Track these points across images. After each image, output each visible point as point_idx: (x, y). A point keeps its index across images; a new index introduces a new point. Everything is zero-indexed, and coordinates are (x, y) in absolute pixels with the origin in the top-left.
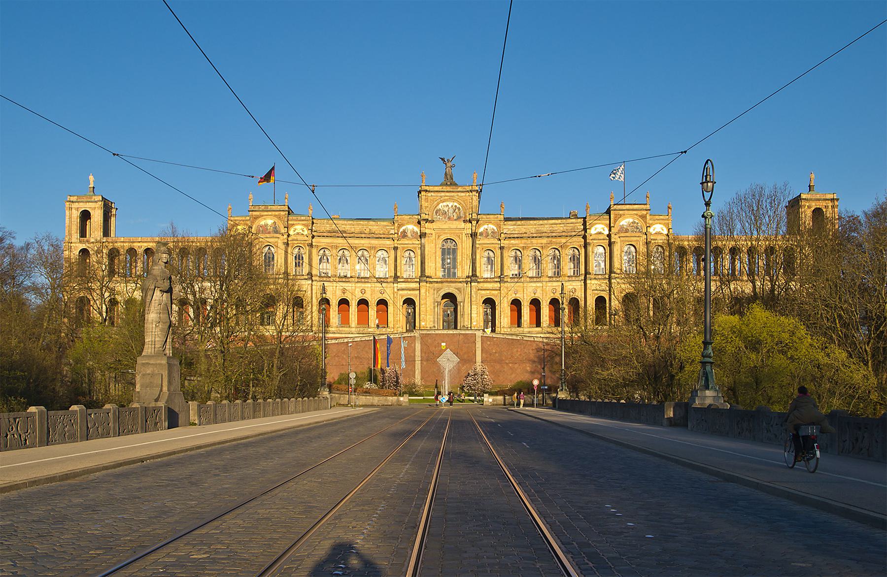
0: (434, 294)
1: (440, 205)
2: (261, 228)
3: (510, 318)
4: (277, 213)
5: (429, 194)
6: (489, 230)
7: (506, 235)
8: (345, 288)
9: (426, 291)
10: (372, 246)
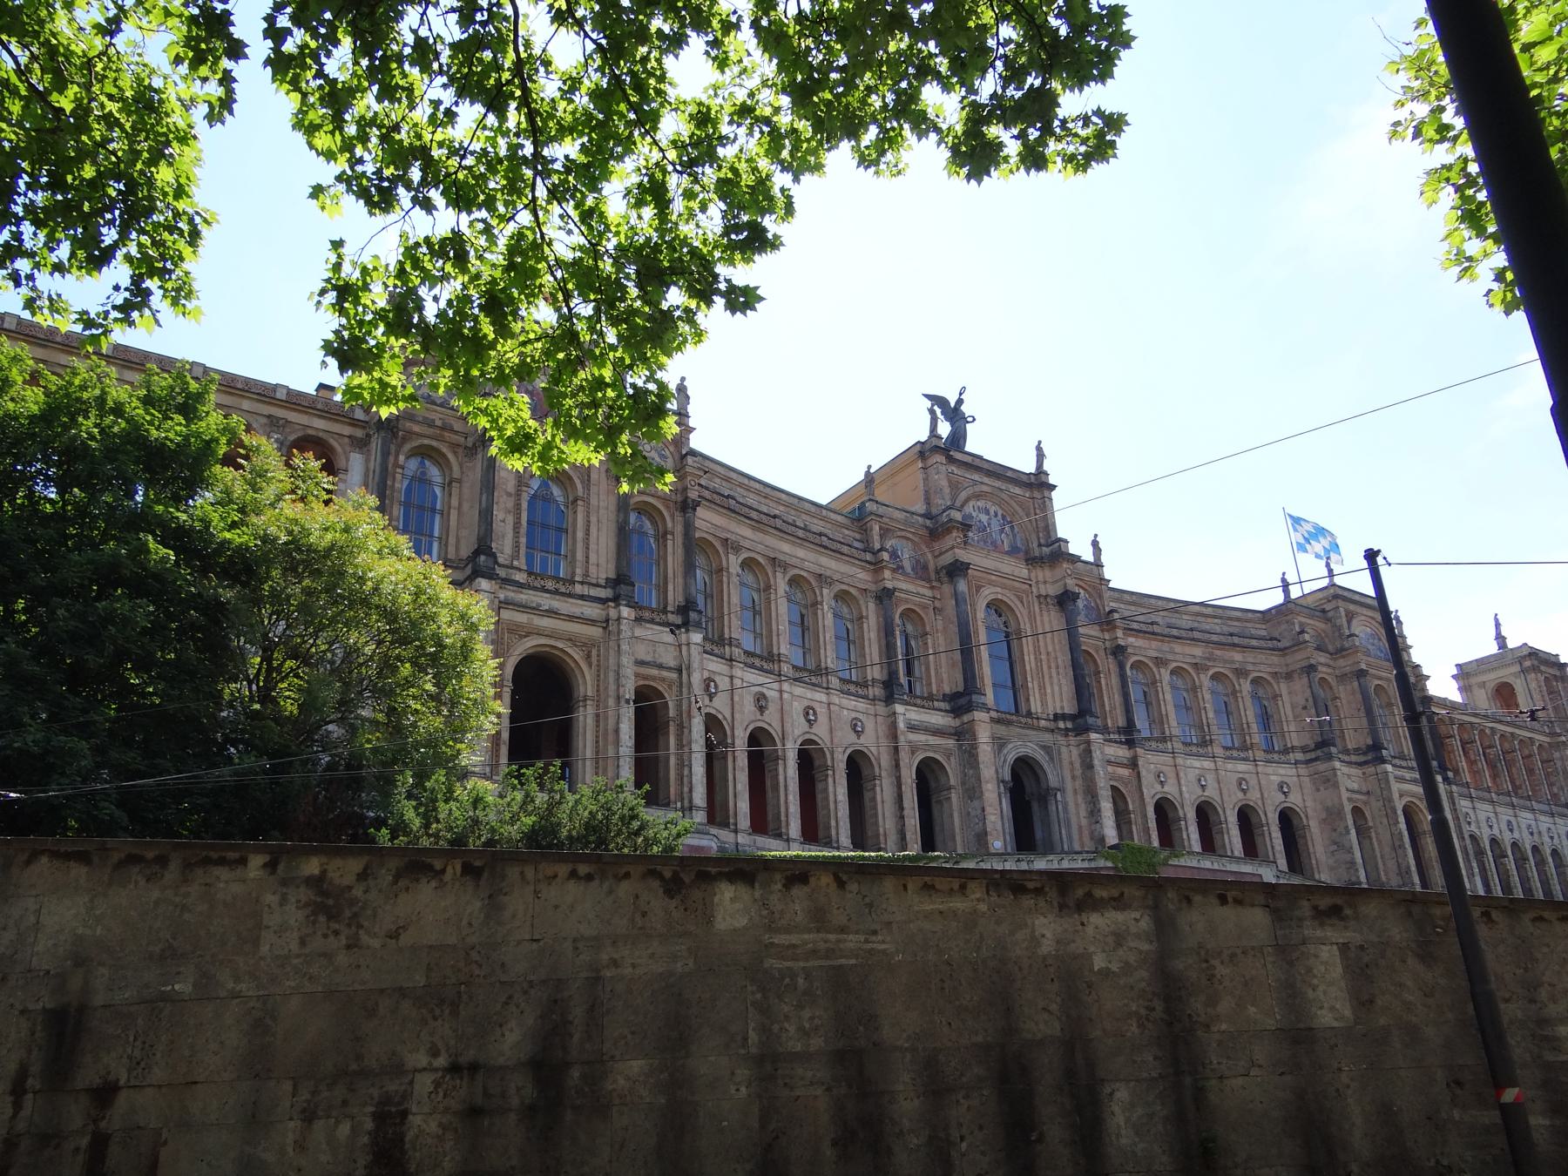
1: (971, 503)
5: (953, 468)
8: (765, 691)
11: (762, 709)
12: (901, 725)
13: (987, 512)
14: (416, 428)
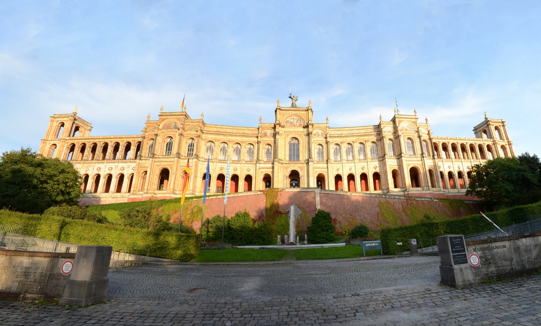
0: (284, 171)
2: (166, 126)
4: (178, 117)
8: (223, 166)
10: (243, 141)
11: (221, 170)
12: (257, 168)
14: (149, 136)
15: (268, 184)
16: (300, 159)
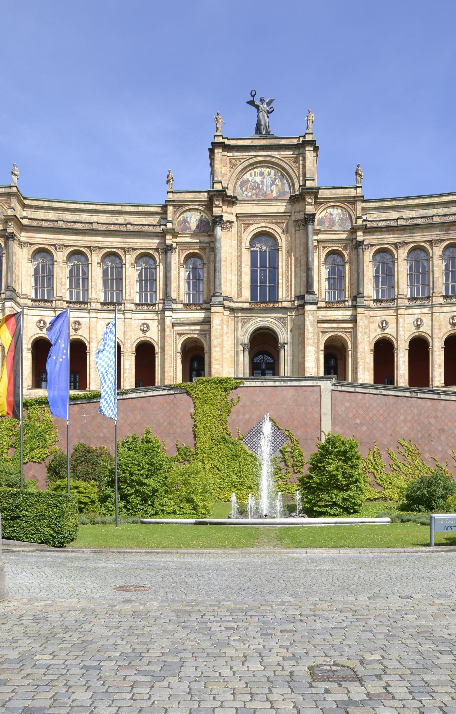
1: (249, 173)
3: (373, 372)
6: (335, 216)
7: (365, 223)
8: (80, 320)
9: (223, 323)
10: (127, 245)
12: (168, 322)
13: (262, 174)
15: (196, 365)
16: (280, 296)
